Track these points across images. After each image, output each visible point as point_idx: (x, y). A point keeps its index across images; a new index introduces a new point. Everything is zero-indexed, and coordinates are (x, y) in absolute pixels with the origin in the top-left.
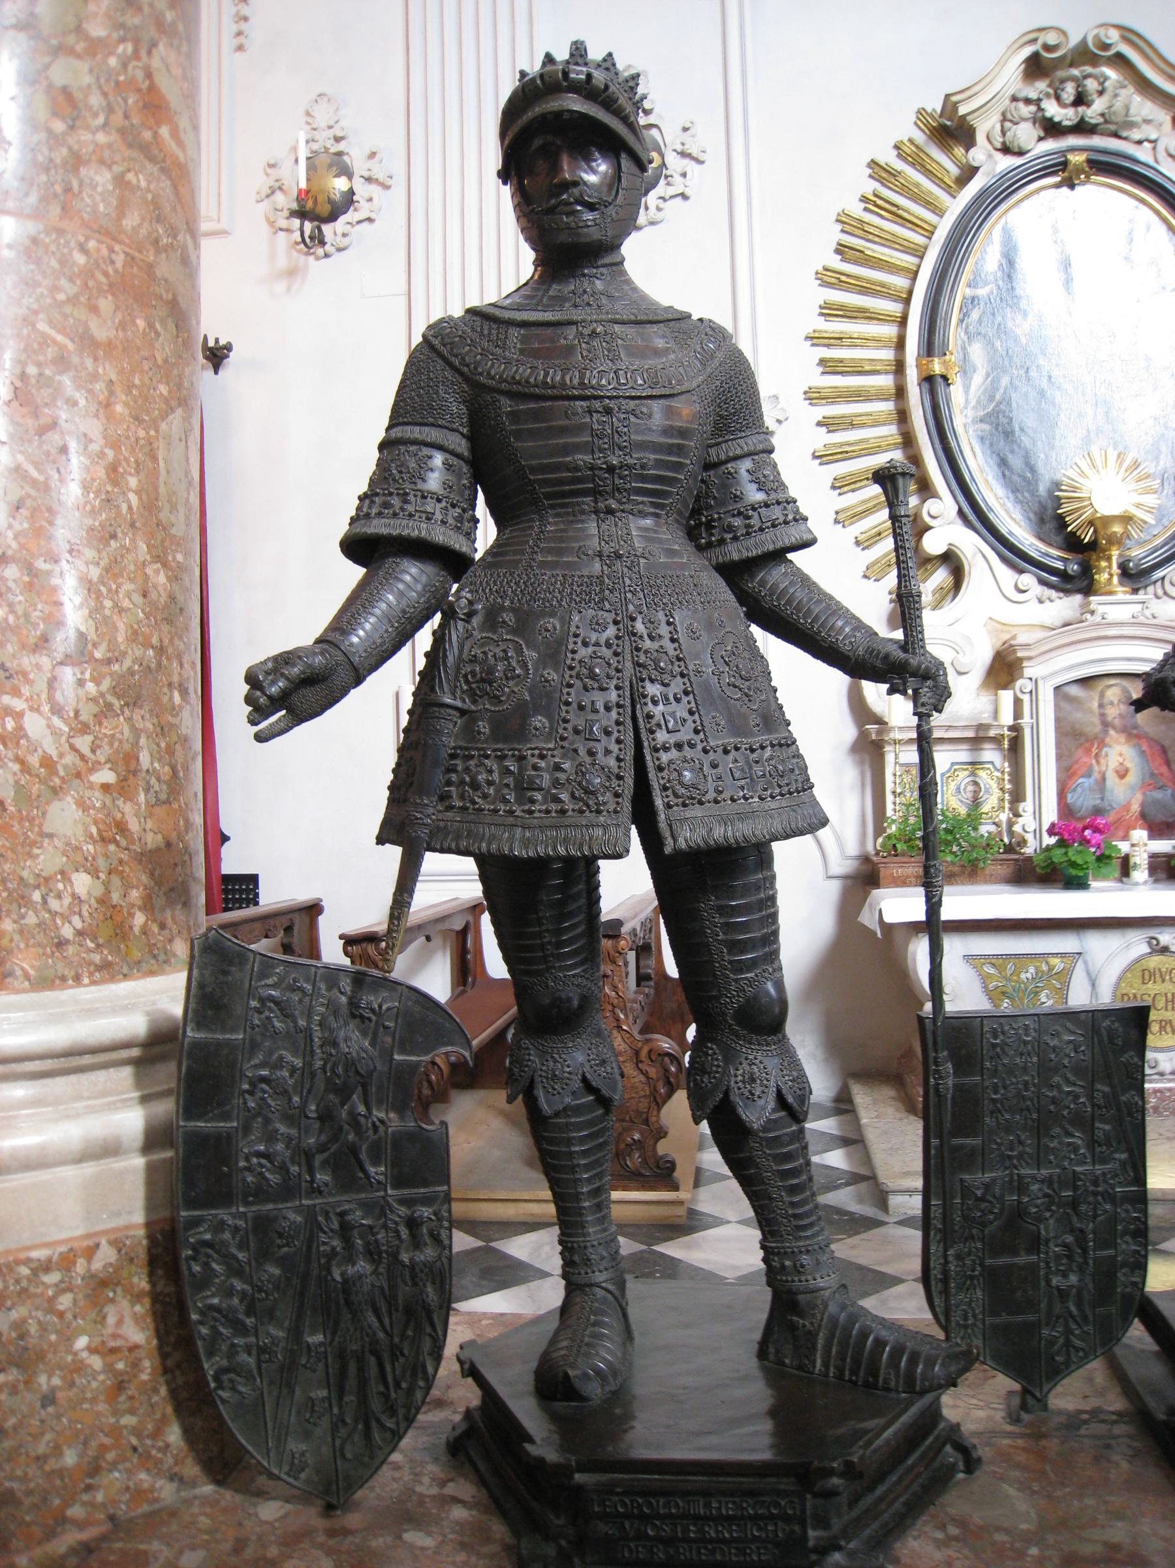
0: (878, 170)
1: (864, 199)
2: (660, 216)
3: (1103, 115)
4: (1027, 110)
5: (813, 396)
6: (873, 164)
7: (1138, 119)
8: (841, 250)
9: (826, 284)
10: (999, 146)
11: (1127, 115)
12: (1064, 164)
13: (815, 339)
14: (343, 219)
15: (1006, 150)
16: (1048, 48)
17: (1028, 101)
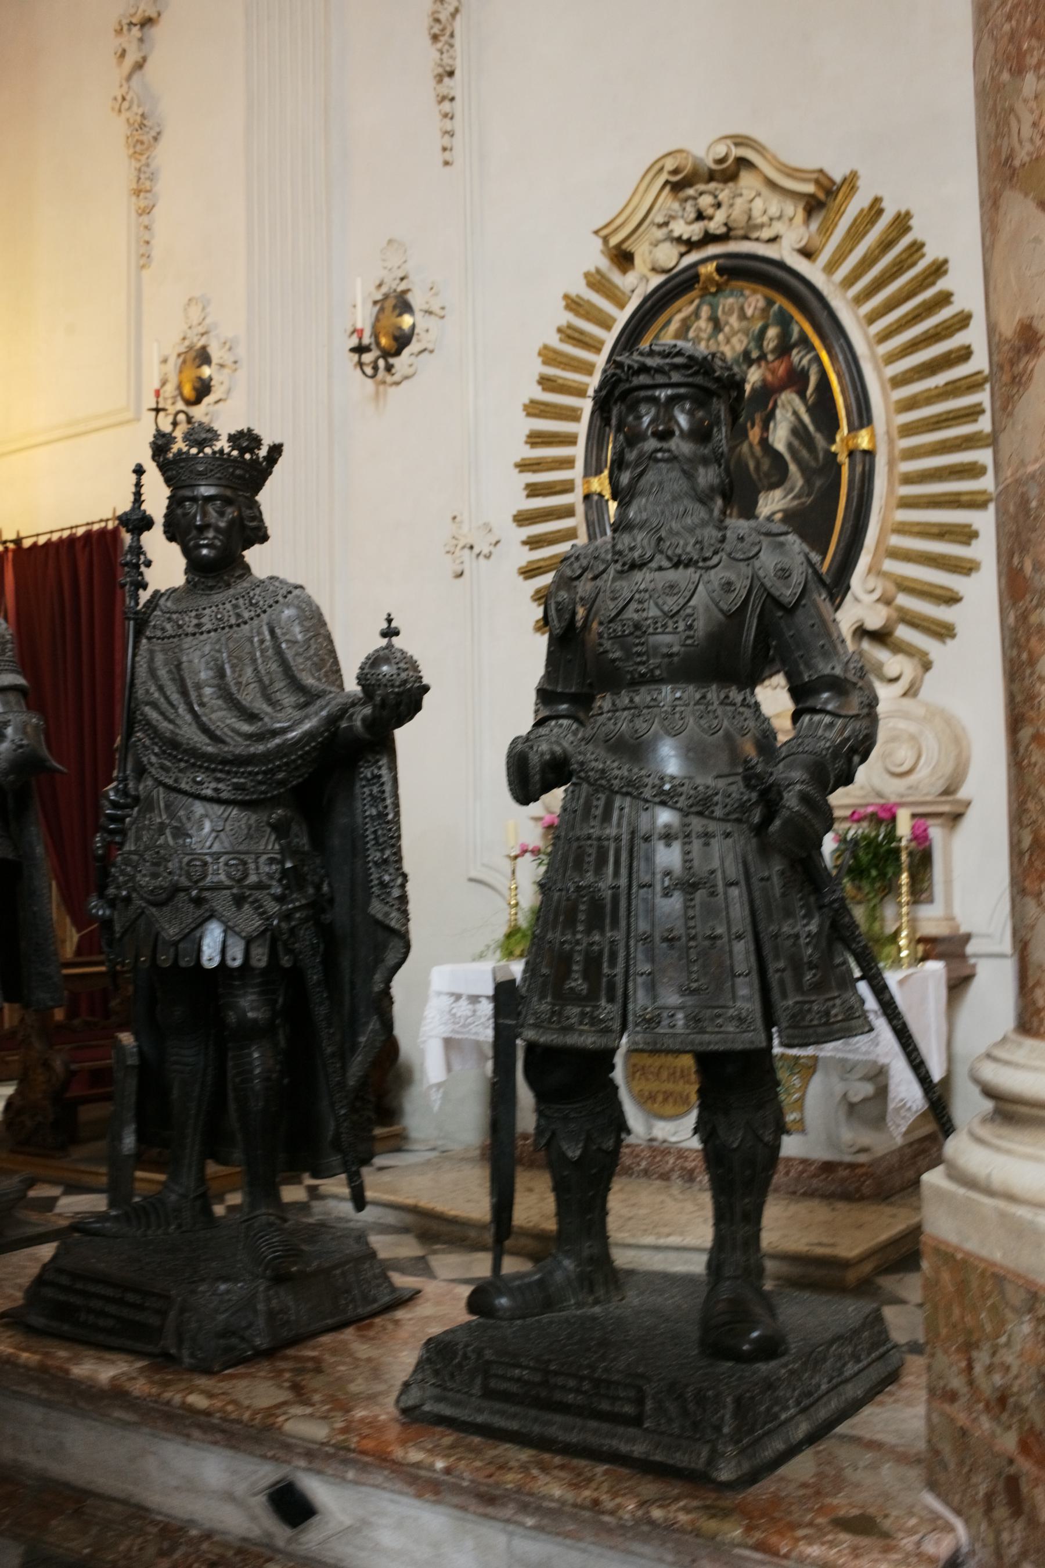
0: (574, 304)
1: (560, 330)
2: (410, 371)
3: (726, 224)
4: (661, 233)
5: (523, 519)
6: (566, 297)
7: (765, 219)
8: (545, 382)
9: (529, 415)
10: (650, 266)
11: (750, 218)
12: (696, 277)
13: (524, 466)
14: (207, 400)
15: (654, 270)
16: (675, 172)
17: (660, 226)
